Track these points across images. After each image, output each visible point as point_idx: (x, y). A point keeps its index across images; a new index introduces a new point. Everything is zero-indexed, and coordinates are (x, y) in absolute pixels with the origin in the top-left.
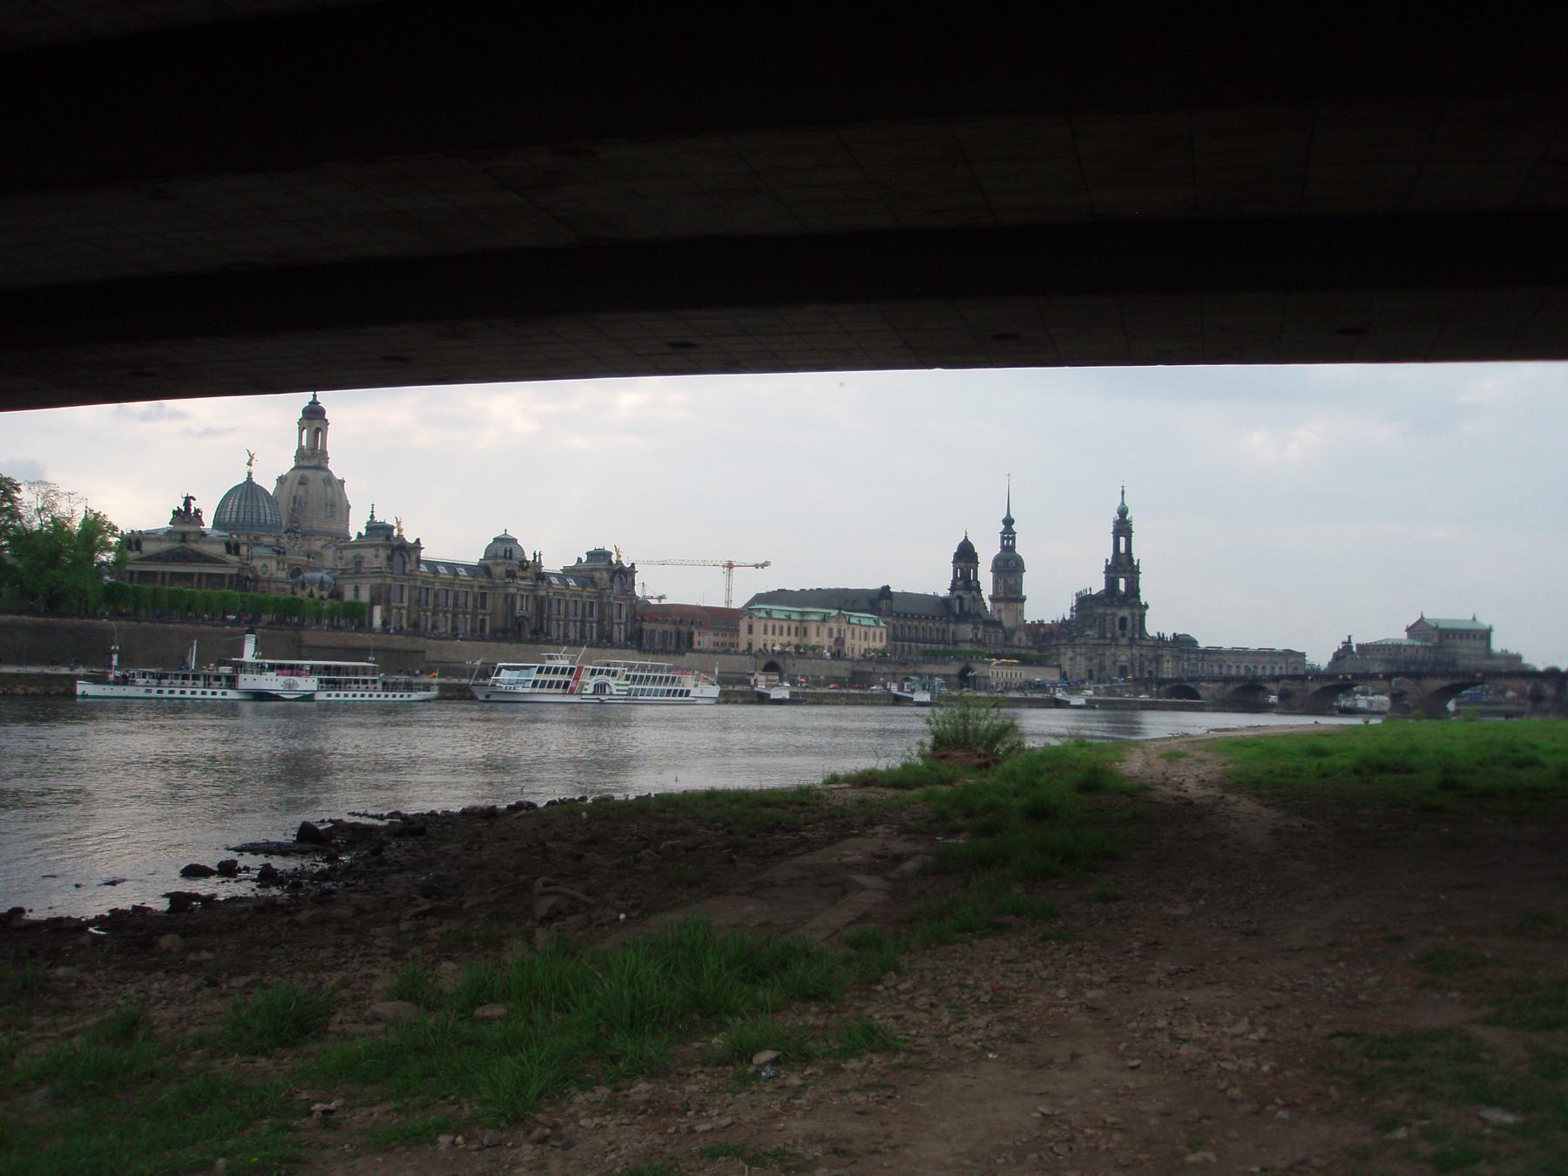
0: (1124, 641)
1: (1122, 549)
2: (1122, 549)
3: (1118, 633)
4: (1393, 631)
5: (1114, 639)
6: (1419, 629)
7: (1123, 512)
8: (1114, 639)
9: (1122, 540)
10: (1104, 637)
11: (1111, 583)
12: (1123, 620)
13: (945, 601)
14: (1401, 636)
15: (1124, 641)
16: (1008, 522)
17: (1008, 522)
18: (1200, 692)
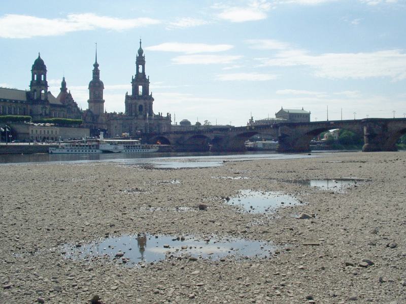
0: (141, 117)
1: (141, 71)
2: (141, 71)
3: (138, 113)
4: (272, 116)
5: (136, 115)
6: (281, 113)
7: (141, 52)
8: (136, 115)
9: (141, 67)
10: (132, 116)
11: (135, 90)
12: (141, 107)
13: (28, 94)
14: (274, 117)
15: (141, 117)
16: (96, 65)
17: (96, 65)
18: (170, 140)
